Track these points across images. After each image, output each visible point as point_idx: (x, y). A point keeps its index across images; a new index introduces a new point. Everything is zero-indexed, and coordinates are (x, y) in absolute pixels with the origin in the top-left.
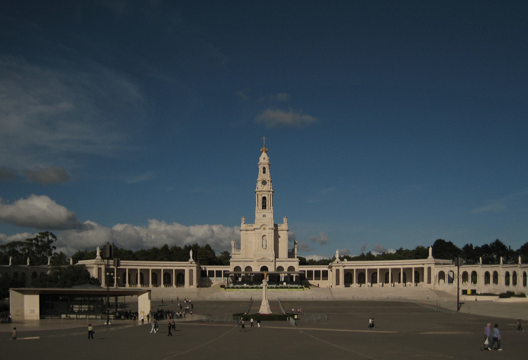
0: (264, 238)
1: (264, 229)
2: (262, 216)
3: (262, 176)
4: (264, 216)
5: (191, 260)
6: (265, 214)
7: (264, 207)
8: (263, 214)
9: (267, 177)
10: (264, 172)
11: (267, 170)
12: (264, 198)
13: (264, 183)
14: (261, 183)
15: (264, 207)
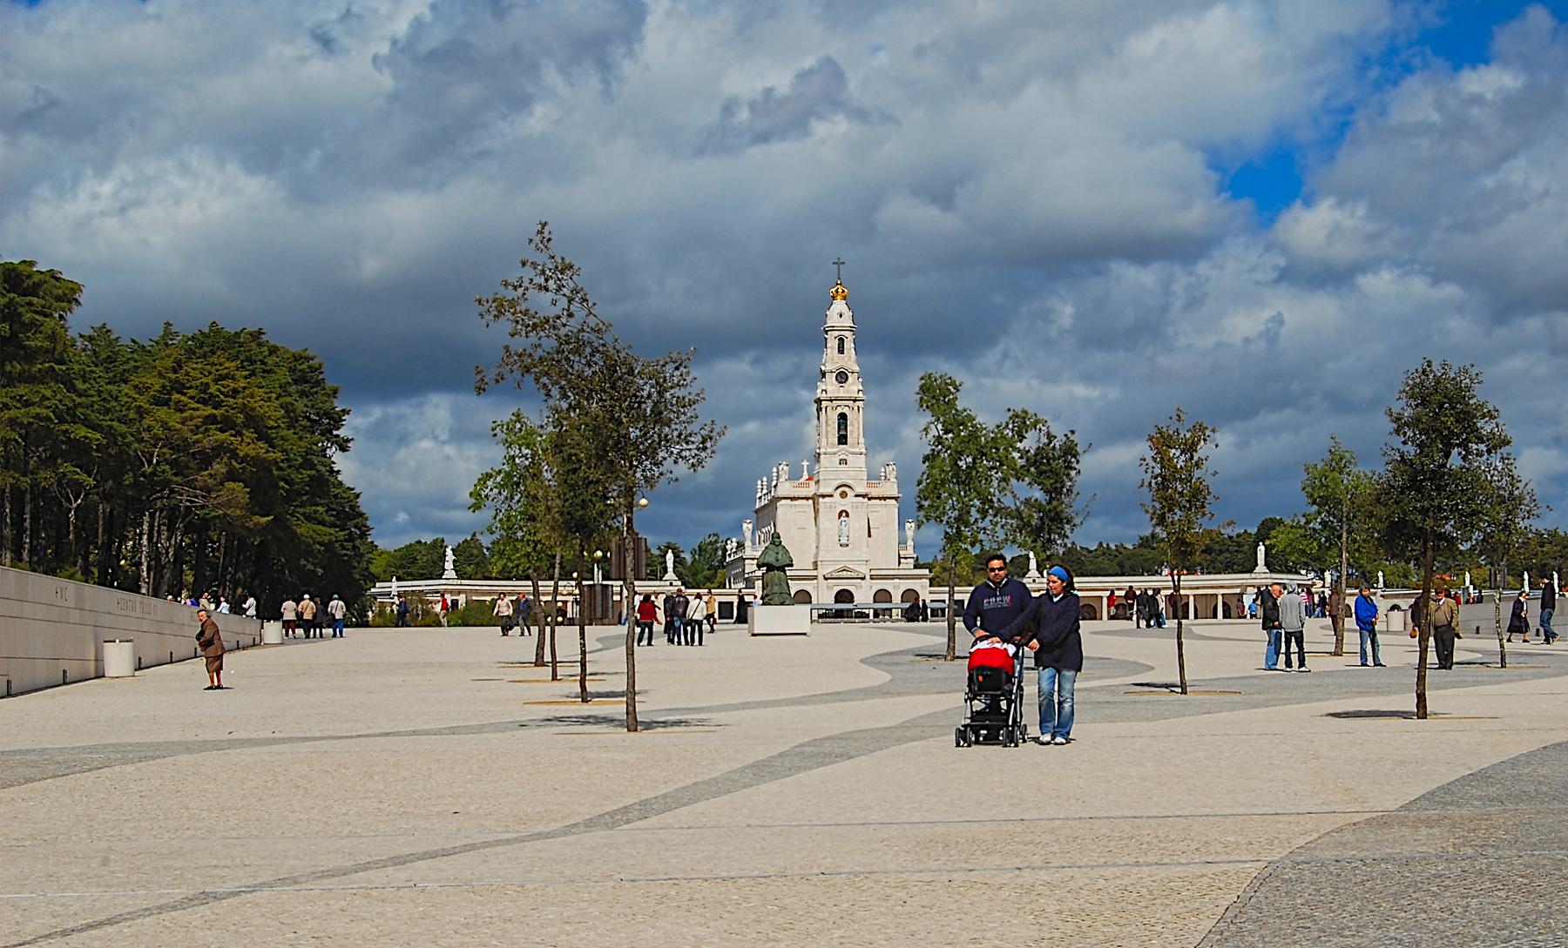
0: (842, 518)
1: (844, 495)
2: (838, 462)
3: (836, 359)
4: (843, 462)
5: (670, 575)
6: (846, 457)
7: (843, 440)
8: (841, 457)
9: (850, 361)
10: (841, 351)
11: (849, 345)
12: (843, 417)
13: (842, 377)
14: (834, 378)
15: (843, 440)
